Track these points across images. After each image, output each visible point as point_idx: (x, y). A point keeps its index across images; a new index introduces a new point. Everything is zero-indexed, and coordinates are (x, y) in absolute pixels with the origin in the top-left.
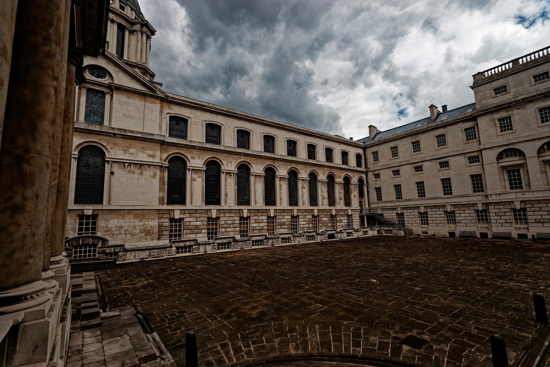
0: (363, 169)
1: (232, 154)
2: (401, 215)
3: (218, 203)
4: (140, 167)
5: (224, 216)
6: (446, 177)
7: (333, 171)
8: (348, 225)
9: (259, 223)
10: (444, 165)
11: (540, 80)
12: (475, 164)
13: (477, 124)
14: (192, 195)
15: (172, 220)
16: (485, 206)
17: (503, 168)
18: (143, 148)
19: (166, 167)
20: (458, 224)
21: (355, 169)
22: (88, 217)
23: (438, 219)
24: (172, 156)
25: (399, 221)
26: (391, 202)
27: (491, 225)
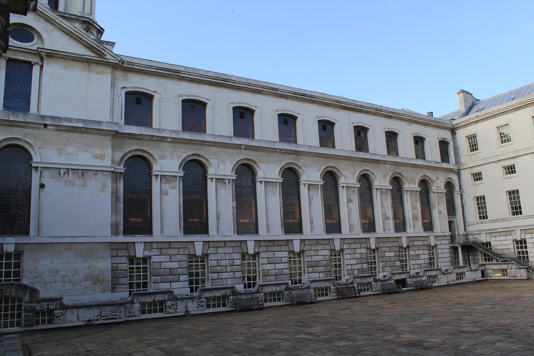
0: (452, 164)
1: (225, 147)
2: (521, 243)
3: (205, 230)
4: (82, 174)
7: (401, 170)
8: (430, 263)
9: (275, 264)
14: (162, 219)
15: (132, 260)
18: (86, 145)
19: (121, 173)
21: (438, 166)
24: (130, 155)
25: (519, 252)
26: (503, 220)
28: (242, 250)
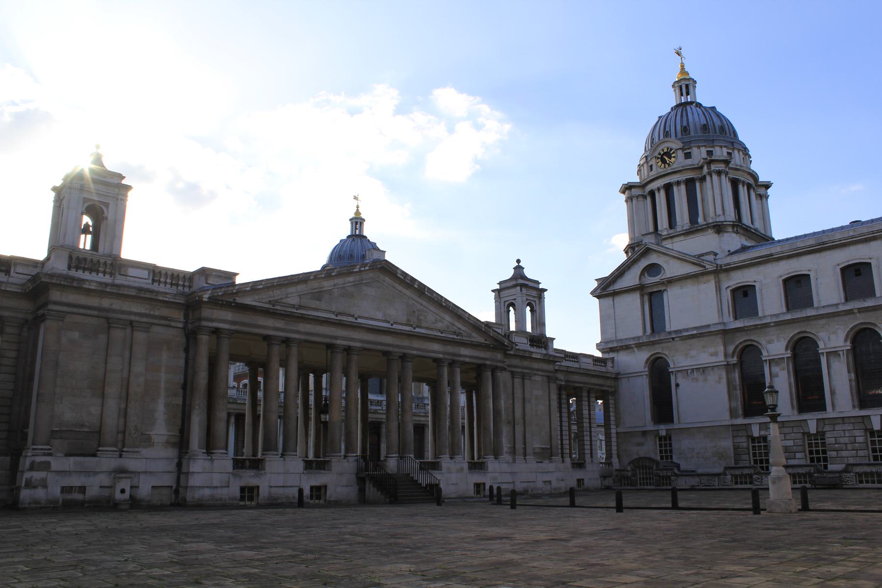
4: (703, 371)
5: (832, 429)
19: (734, 364)
22: (665, 438)
24: (741, 346)
28: (865, 426)
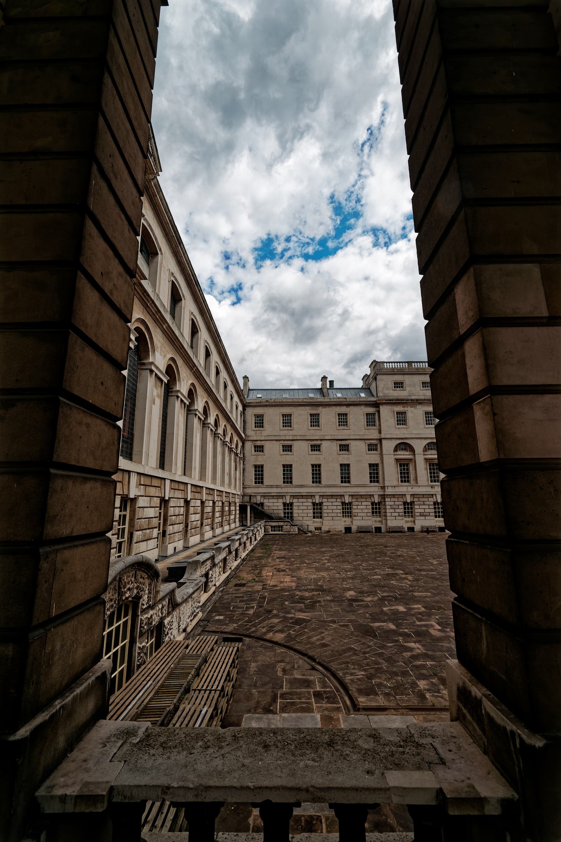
6: (345, 462)
10: (345, 448)
11: (425, 387)
12: (373, 452)
13: (379, 412)
16: (381, 498)
17: (397, 460)
20: (355, 518)
23: (334, 511)
27: (387, 518)
